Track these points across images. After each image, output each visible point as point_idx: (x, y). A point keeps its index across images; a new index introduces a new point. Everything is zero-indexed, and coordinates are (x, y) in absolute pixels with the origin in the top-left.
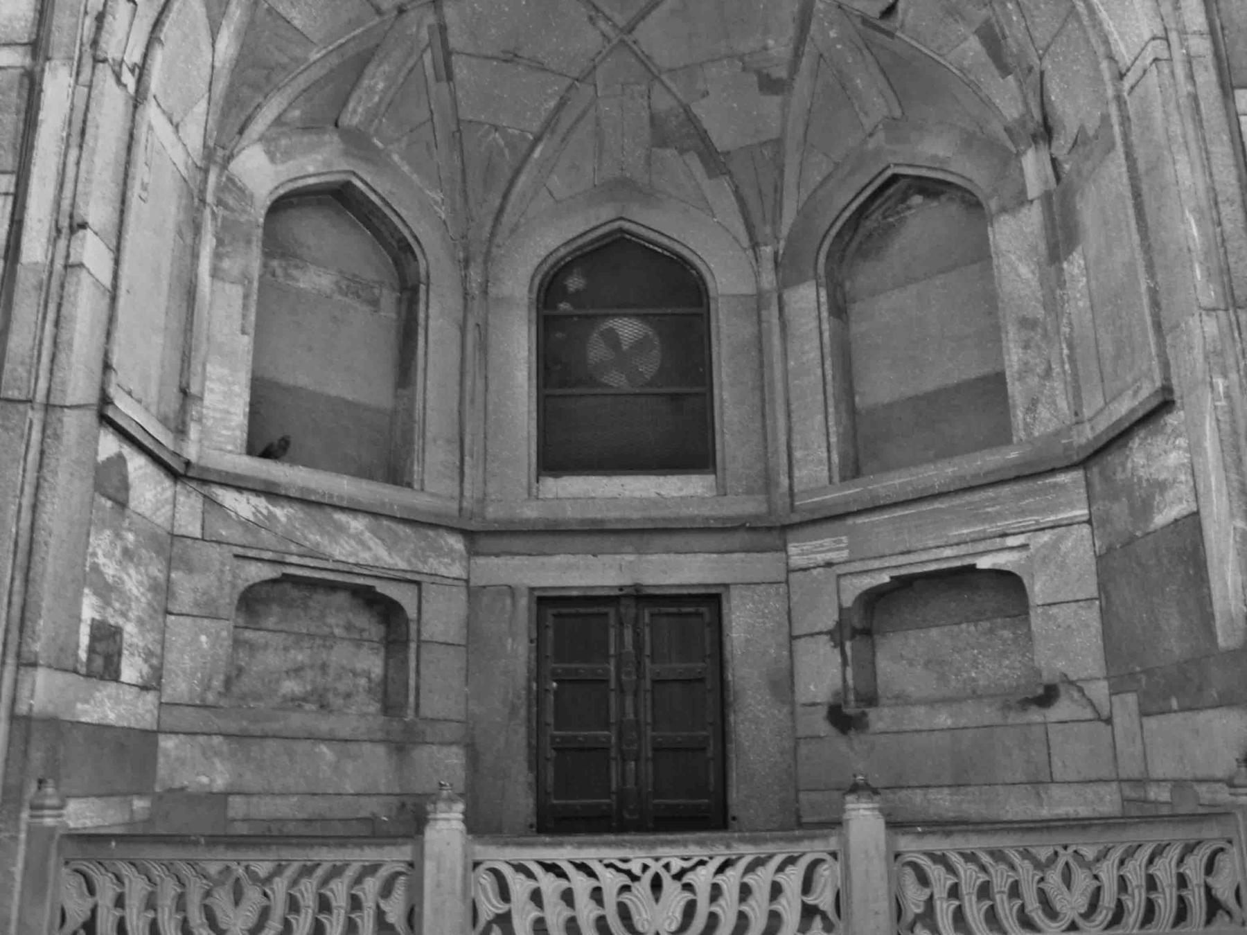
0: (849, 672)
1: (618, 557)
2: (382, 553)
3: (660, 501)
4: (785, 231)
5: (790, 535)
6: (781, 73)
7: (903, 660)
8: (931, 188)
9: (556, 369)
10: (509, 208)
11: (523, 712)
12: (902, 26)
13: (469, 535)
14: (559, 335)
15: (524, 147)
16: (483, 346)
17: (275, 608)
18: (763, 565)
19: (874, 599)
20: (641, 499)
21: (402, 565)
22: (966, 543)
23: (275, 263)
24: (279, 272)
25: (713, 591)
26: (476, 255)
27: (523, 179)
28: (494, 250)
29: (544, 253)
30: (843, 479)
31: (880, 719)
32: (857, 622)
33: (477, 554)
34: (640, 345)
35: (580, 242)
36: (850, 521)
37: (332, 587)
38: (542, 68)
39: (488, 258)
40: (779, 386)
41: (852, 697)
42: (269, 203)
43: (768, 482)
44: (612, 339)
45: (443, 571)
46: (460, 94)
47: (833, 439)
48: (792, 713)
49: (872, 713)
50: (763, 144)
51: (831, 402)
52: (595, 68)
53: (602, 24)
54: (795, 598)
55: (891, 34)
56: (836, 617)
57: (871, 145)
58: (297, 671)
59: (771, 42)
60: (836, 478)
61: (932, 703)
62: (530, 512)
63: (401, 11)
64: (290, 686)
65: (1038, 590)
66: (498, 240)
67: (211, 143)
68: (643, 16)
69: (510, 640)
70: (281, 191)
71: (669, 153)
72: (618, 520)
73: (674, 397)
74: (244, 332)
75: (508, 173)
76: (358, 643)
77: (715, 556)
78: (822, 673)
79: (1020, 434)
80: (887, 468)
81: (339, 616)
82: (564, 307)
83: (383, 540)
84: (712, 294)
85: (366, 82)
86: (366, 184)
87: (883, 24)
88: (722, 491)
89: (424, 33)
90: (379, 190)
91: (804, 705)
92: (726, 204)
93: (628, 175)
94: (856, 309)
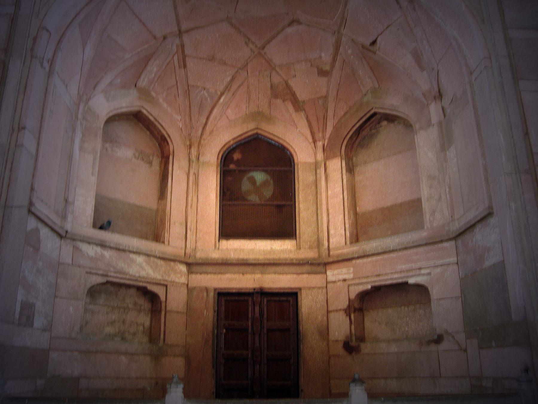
0: (353, 327)
1: (253, 276)
2: (151, 272)
3: (272, 251)
4: (328, 135)
5: (327, 267)
6: (327, 68)
7: (377, 322)
8: (390, 118)
9: (228, 193)
10: (209, 123)
11: (210, 343)
12: (379, 48)
13: (189, 265)
14: (230, 179)
15: (216, 97)
16: (197, 183)
17: (103, 296)
18: (316, 280)
19: (364, 296)
20: (264, 251)
21: (159, 277)
22: (404, 271)
23: (107, 145)
24: (109, 149)
25: (295, 291)
26: (194, 143)
27: (215, 111)
28: (202, 141)
29: (224, 143)
30: (351, 243)
31: (366, 348)
32: (356, 305)
33: (192, 273)
34: (265, 184)
35: (239, 138)
36: (354, 262)
37: (128, 286)
38: (225, 64)
39: (199, 143)
40: (324, 202)
41: (354, 338)
42: (105, 119)
43: (319, 243)
44: (253, 181)
45: (177, 280)
46: (189, 74)
47: (347, 226)
48: (328, 344)
49: (362, 346)
50: (319, 98)
51: (346, 209)
52: (247, 64)
53: (251, 45)
54: (330, 295)
55: (375, 53)
56: (347, 303)
57: (365, 99)
58: (112, 323)
59: (323, 55)
60: (348, 242)
61: (388, 341)
62: (215, 255)
63: (165, 38)
64: (109, 330)
65: (434, 293)
66: (204, 136)
67: (81, 93)
68: (268, 42)
69: (206, 311)
70: (111, 114)
71: (279, 101)
72: (255, 260)
73: (279, 207)
74: (93, 174)
75: (209, 109)
76: (140, 311)
77: (295, 276)
78: (340, 327)
79: (427, 225)
80: (370, 238)
81: (132, 299)
82: (232, 166)
83: (151, 267)
84: (296, 161)
85: (148, 68)
86: (148, 112)
87: (371, 48)
88: (299, 247)
89: (175, 47)
90: (153, 114)
91: (333, 341)
92: (302, 124)
93: (261, 110)
94: (357, 170)
